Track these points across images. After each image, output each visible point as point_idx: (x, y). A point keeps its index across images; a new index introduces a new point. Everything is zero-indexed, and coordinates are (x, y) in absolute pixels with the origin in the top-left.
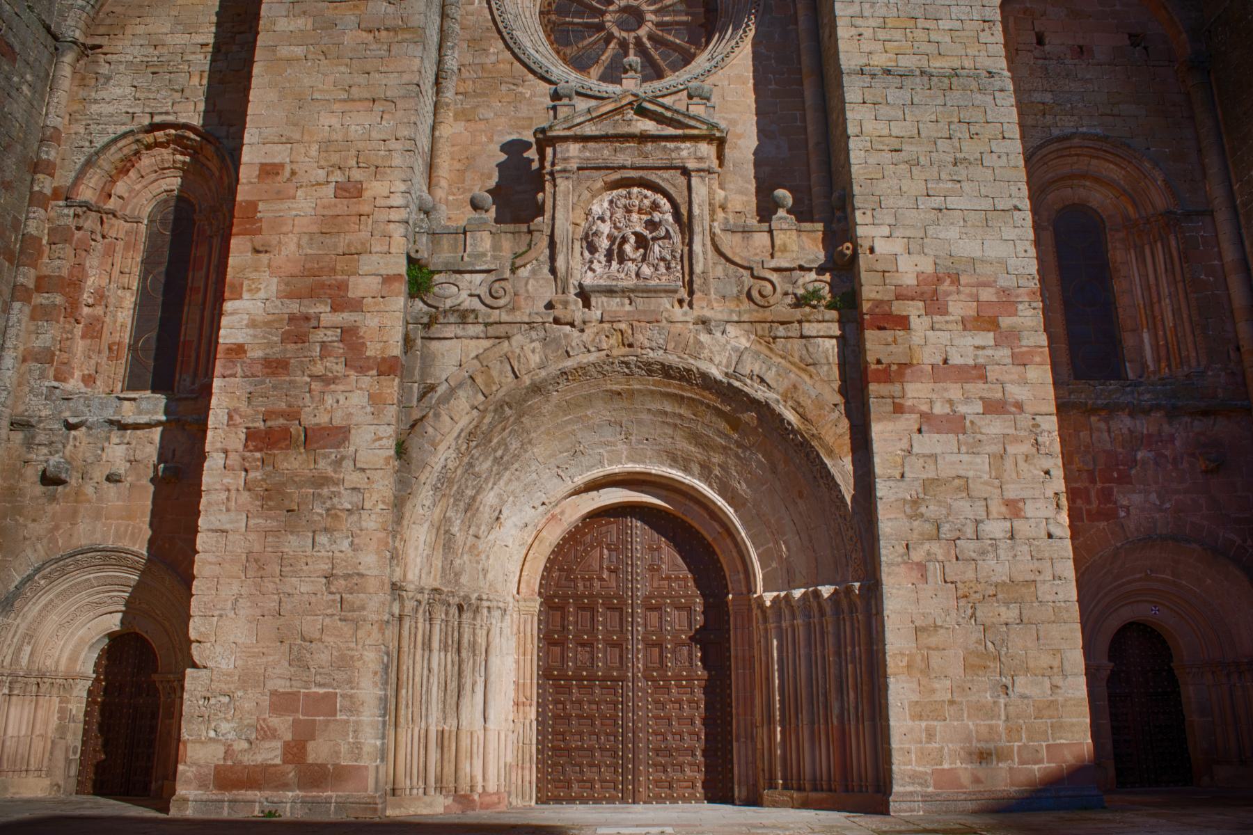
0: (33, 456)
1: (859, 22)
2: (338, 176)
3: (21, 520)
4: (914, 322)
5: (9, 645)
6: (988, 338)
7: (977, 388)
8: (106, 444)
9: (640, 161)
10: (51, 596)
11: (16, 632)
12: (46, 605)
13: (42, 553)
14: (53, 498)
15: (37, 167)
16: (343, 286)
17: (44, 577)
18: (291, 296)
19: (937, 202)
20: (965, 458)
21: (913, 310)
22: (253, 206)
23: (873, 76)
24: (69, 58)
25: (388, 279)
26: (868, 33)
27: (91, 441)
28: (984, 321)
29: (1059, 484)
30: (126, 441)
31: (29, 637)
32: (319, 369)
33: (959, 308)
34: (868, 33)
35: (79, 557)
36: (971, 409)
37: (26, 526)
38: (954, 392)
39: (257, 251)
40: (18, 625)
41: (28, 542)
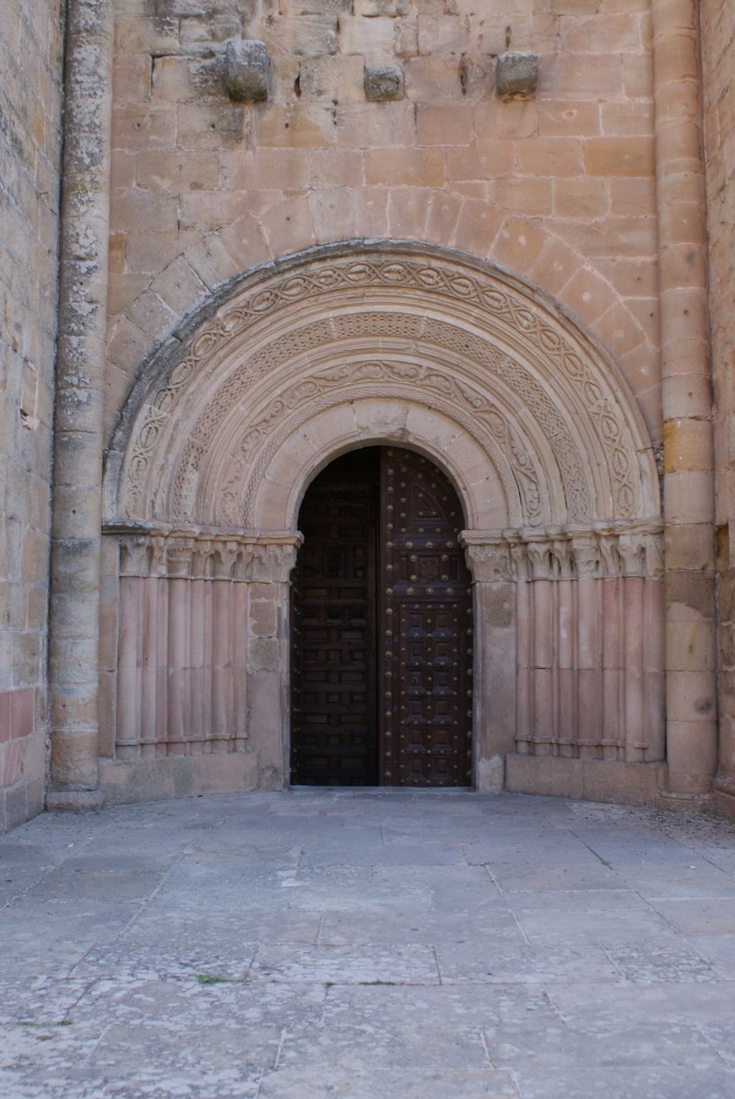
0: (169, 42)
3: (165, 184)
5: (162, 468)
8: (345, 15)
10: (242, 360)
11: (172, 439)
12: (230, 381)
13: (227, 259)
14: (234, 135)
17: (235, 315)
27: (310, 8)
30: (392, 8)
31: (197, 451)
35: (315, 267)
37: (178, 197)
40: (177, 425)
41: (188, 235)
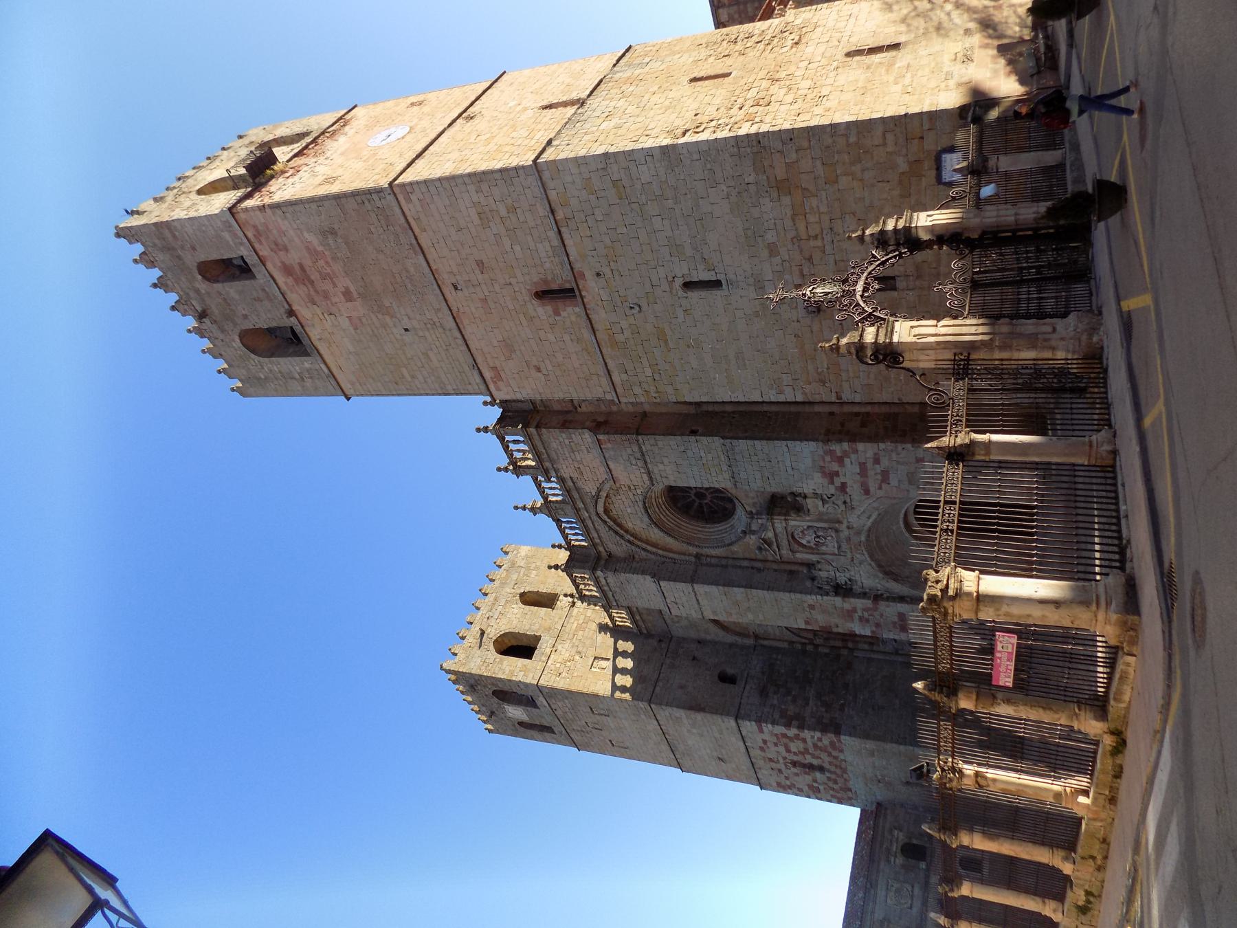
1: (710, 480)
2: (808, 609)
4: (843, 480)
6: (847, 461)
7: (869, 465)
9: (785, 537)
15: (804, 652)
16: (848, 611)
18: (853, 620)
19: (789, 470)
20: (899, 472)
21: (838, 481)
22: (820, 627)
23: (736, 482)
24: (762, 642)
25: (844, 601)
26: (715, 479)
28: (840, 460)
29: (909, 446)
32: (878, 617)
33: (835, 467)
34: (715, 479)
36: (878, 468)
38: (871, 473)
39: (837, 627)
